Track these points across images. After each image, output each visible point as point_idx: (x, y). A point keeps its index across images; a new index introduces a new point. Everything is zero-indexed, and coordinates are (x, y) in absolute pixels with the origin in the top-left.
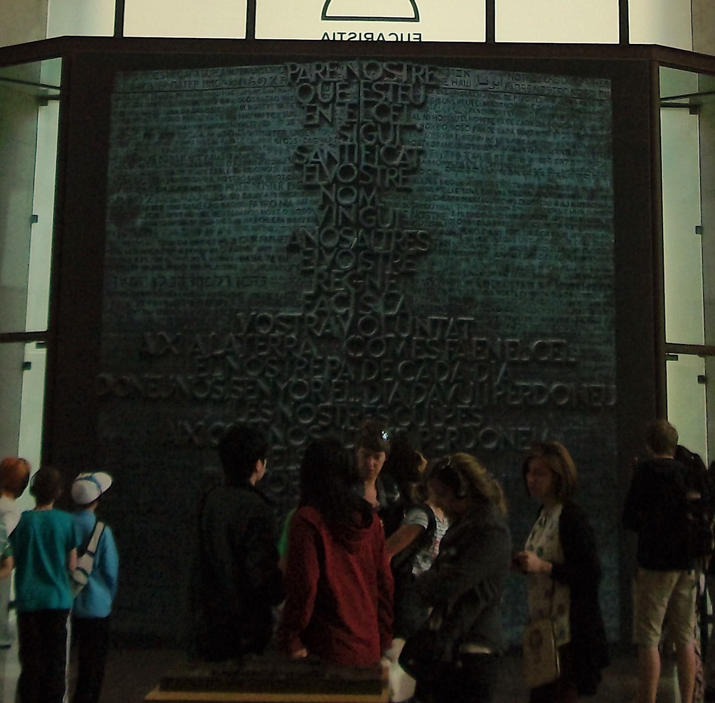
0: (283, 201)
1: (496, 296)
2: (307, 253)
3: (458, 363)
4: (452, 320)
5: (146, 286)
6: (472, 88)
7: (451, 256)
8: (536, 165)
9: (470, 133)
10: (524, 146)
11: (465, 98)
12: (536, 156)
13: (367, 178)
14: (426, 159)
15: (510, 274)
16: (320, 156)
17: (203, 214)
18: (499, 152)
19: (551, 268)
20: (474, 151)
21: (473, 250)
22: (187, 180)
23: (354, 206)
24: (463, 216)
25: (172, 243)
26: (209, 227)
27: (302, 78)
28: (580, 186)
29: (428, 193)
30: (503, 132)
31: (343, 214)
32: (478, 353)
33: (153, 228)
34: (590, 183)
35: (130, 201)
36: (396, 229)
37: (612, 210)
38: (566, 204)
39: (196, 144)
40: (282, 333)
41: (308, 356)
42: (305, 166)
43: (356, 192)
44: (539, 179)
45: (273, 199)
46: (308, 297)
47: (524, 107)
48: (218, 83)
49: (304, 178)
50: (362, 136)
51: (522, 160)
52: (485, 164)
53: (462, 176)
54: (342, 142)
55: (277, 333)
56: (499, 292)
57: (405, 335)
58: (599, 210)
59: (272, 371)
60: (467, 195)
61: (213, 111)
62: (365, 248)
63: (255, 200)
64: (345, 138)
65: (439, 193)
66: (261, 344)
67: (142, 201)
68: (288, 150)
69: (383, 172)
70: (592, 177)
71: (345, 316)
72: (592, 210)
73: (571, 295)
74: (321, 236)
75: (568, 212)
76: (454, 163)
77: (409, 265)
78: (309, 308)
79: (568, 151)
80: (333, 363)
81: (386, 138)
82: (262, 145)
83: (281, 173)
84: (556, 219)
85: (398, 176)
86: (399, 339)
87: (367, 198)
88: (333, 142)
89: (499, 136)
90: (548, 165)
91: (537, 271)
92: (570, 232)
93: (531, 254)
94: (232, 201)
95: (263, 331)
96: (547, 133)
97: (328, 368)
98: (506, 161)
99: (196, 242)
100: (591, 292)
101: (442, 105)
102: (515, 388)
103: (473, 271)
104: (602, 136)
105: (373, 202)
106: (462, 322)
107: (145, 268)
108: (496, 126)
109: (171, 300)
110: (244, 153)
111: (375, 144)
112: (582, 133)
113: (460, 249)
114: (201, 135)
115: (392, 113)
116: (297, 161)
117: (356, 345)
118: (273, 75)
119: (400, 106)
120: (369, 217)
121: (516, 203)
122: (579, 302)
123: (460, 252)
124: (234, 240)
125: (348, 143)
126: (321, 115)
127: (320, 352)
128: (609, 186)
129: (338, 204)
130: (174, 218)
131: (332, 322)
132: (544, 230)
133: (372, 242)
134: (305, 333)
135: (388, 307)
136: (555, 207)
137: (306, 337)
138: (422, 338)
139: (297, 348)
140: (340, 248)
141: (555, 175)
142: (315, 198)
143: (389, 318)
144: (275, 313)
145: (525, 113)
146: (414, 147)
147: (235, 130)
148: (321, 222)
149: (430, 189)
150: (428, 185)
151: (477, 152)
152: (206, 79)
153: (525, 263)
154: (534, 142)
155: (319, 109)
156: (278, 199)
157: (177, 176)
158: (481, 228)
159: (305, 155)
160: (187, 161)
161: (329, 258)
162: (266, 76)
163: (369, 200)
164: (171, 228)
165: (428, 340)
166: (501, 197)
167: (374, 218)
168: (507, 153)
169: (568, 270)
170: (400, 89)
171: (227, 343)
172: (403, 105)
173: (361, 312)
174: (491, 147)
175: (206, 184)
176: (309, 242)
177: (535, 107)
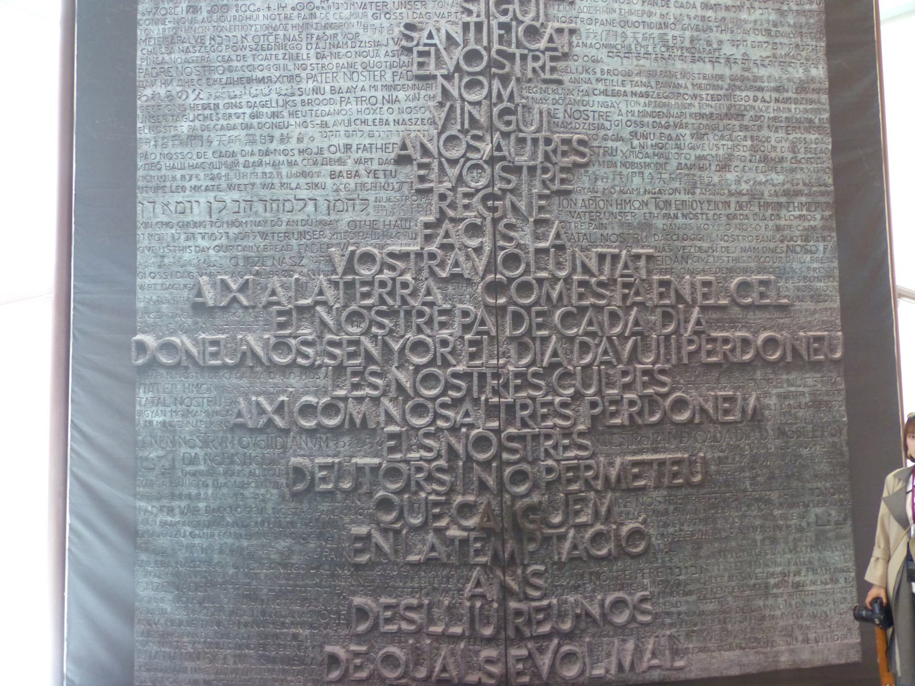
0: (387, 97)
1: (681, 221)
2: (421, 166)
3: (635, 309)
4: (624, 252)
5: (198, 213)
7: (619, 169)
8: (727, 50)
10: (710, 24)
12: (725, 37)
13: (502, 66)
14: (580, 42)
15: (698, 191)
16: (435, 36)
17: (274, 115)
18: (677, 33)
19: (751, 183)
21: (648, 160)
22: (251, 68)
23: (485, 103)
24: (633, 115)
25: (233, 154)
26: (285, 132)
28: (785, 77)
29: (585, 87)
31: (470, 113)
32: (661, 296)
33: (206, 134)
34: (798, 73)
35: (170, 97)
36: (543, 133)
37: (827, 107)
38: (768, 99)
40: (392, 274)
41: (431, 304)
42: (415, 50)
43: (485, 82)
44: (731, 68)
45: (373, 93)
46: (427, 225)
49: (415, 65)
50: (492, 8)
51: (709, 43)
52: (660, 49)
53: (629, 64)
55: (387, 275)
56: (684, 216)
57: (563, 274)
58: (810, 107)
59: (381, 326)
60: (638, 89)
62: (503, 158)
63: (348, 94)
64: (470, 12)
65: (601, 86)
66: (365, 289)
67: (187, 97)
68: (391, 29)
69: (524, 57)
70: (798, 65)
71: (478, 250)
72: (802, 107)
73: (779, 217)
74: (441, 143)
75: (771, 110)
76: (619, 47)
77: (563, 181)
78: (428, 238)
79: (768, 32)
80: (465, 314)
81: (525, 13)
82: (354, 21)
83: (383, 59)
84: (758, 118)
86: (555, 279)
87: (503, 93)
88: (452, 18)
89: (678, 11)
90: (742, 50)
91: (733, 187)
92: (773, 136)
93: (724, 167)
94: (316, 96)
95: (366, 272)
97: (458, 321)
98: (687, 44)
99: (267, 153)
100: (804, 212)
102: (714, 340)
103: (649, 188)
104: (810, 11)
105: (511, 98)
106: (638, 257)
107: (196, 189)
109: (234, 230)
110: (329, 32)
111: (511, 20)
112: (785, 8)
113: (631, 159)
114: (269, 8)
116: (404, 43)
117: (494, 288)
120: (507, 118)
121: (702, 99)
122: (790, 227)
123: (632, 164)
124: (320, 151)
125: (473, 19)
127: (446, 298)
128: (822, 76)
129: (463, 99)
130: (234, 121)
131: (462, 259)
133: (512, 150)
134: (425, 273)
135: (537, 238)
136: (754, 104)
137: (426, 279)
138: (587, 278)
139: (414, 294)
140: (468, 159)
141: (751, 65)
142: (431, 93)
143: (538, 251)
144: (381, 247)
146: (564, 25)
148: (440, 123)
149: (589, 81)
150: (584, 76)
151: (649, 31)
153: (716, 179)
154: (724, 19)
156: (379, 94)
157: (235, 64)
158: (658, 131)
159: (415, 35)
160: (249, 42)
161: (453, 172)
163: (506, 94)
164: (234, 133)
165: (594, 280)
167: (513, 118)
168: (688, 34)
169: (773, 185)
171: (316, 290)
173: (501, 243)
174: (666, 25)
175: (277, 74)
176: (425, 151)
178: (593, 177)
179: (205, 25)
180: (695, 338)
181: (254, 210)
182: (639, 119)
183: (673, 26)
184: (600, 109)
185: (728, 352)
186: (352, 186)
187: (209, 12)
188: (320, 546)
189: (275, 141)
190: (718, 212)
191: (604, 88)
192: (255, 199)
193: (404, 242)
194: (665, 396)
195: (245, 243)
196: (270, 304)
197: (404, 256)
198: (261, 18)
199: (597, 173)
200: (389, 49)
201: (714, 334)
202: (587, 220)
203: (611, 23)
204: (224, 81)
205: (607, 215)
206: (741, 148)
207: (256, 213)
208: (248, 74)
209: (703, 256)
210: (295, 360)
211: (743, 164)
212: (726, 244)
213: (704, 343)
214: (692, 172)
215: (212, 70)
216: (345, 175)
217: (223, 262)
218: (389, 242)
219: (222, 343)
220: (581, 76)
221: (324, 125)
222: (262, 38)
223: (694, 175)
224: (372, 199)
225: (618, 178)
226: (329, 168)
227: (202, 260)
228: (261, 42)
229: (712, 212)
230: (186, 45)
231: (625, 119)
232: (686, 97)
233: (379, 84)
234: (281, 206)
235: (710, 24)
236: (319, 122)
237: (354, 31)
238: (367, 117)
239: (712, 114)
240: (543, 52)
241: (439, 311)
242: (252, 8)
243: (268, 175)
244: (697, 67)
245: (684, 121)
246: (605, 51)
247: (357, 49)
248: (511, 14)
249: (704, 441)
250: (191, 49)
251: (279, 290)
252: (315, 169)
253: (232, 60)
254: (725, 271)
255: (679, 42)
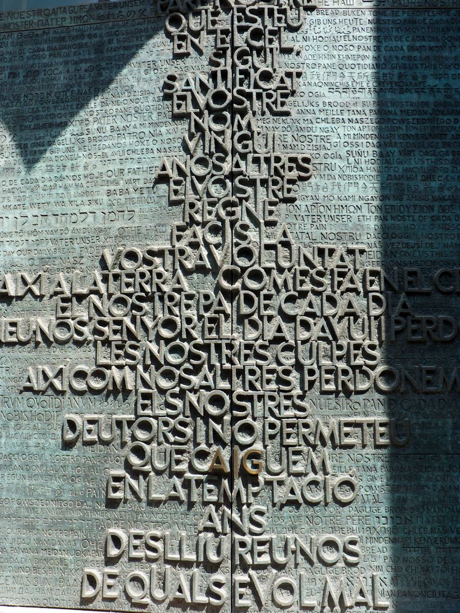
0: (152, 132)
6: (355, 6)
7: (337, 181)
8: (431, 82)
9: (354, 52)
10: (416, 62)
11: (347, 17)
13: (242, 103)
14: (306, 82)
15: (405, 197)
20: (359, 71)
22: (52, 116)
26: (74, 162)
27: (173, 7)
29: (309, 116)
30: (391, 49)
39: (61, 80)
41: (179, 291)
44: (435, 96)
47: (414, 22)
48: (86, 18)
54: (214, 69)
56: (392, 218)
60: (354, 117)
61: (80, 46)
63: (122, 132)
65: (323, 116)
69: (259, 96)
76: (338, 84)
77: (289, 191)
83: (151, 103)
85: (276, 100)
89: (388, 54)
90: (444, 81)
91: (437, 194)
93: (429, 177)
96: (442, 48)
98: (396, 79)
101: (322, 26)
108: (384, 44)
111: (250, 67)
113: (346, 173)
114: (68, 71)
115: (268, 36)
118: (142, 7)
119: (276, 28)
123: (349, 177)
126: (193, 44)
132: (443, 150)
136: (454, 125)
141: (453, 92)
145: (416, 28)
146: (291, 70)
147: (103, 64)
150: (309, 108)
151: (364, 71)
152: (73, 15)
154: (428, 57)
155: (190, 37)
157: (42, 113)
162: (135, 9)
166: (391, 117)
167: (250, 142)
168: (396, 72)
170: (276, 12)
172: (279, 28)
176: (181, 172)
177: (427, 21)
178: (314, 187)
179: (21, 86)
180: (401, 319)
181: (48, 222)
182: (355, 141)
183: (383, 66)
184: (322, 134)
185: (431, 332)
186: (123, 201)
187: (24, 76)
188: (85, 486)
189: (67, 170)
190: (423, 215)
191: (326, 117)
192: (50, 214)
193: (160, 242)
194: (373, 368)
195: (40, 248)
196: (56, 294)
197: (160, 254)
198: (62, 78)
199: (319, 184)
200: (156, 96)
201: (418, 316)
202: (310, 222)
203: (332, 66)
204: (32, 127)
205: (327, 217)
206: (444, 162)
207: (49, 225)
208: (51, 121)
209: (410, 250)
210: (72, 336)
211: (445, 174)
212: (430, 241)
213: (410, 323)
214: (401, 182)
215: (24, 119)
216: (118, 192)
217: (23, 262)
218: (148, 243)
219: (19, 324)
220: (306, 108)
221: (104, 155)
222: (62, 94)
223: (402, 184)
224: (137, 210)
225: (336, 187)
226: (106, 188)
227: (8, 262)
228: (61, 97)
229: (418, 215)
230: (6, 101)
231: (342, 141)
232: (395, 122)
233: (147, 122)
234: (68, 218)
235: (416, 62)
236: (100, 154)
237: (130, 84)
238: (137, 148)
239: (417, 135)
240: (275, 91)
241: (185, 295)
242: (56, 72)
243: (61, 195)
244: (405, 97)
245: (393, 141)
246: (327, 88)
247: (132, 97)
248: (250, 64)
249: (410, 408)
250: (10, 105)
251: (64, 283)
252: (95, 189)
253: (39, 111)
254: (429, 263)
255: (389, 79)
